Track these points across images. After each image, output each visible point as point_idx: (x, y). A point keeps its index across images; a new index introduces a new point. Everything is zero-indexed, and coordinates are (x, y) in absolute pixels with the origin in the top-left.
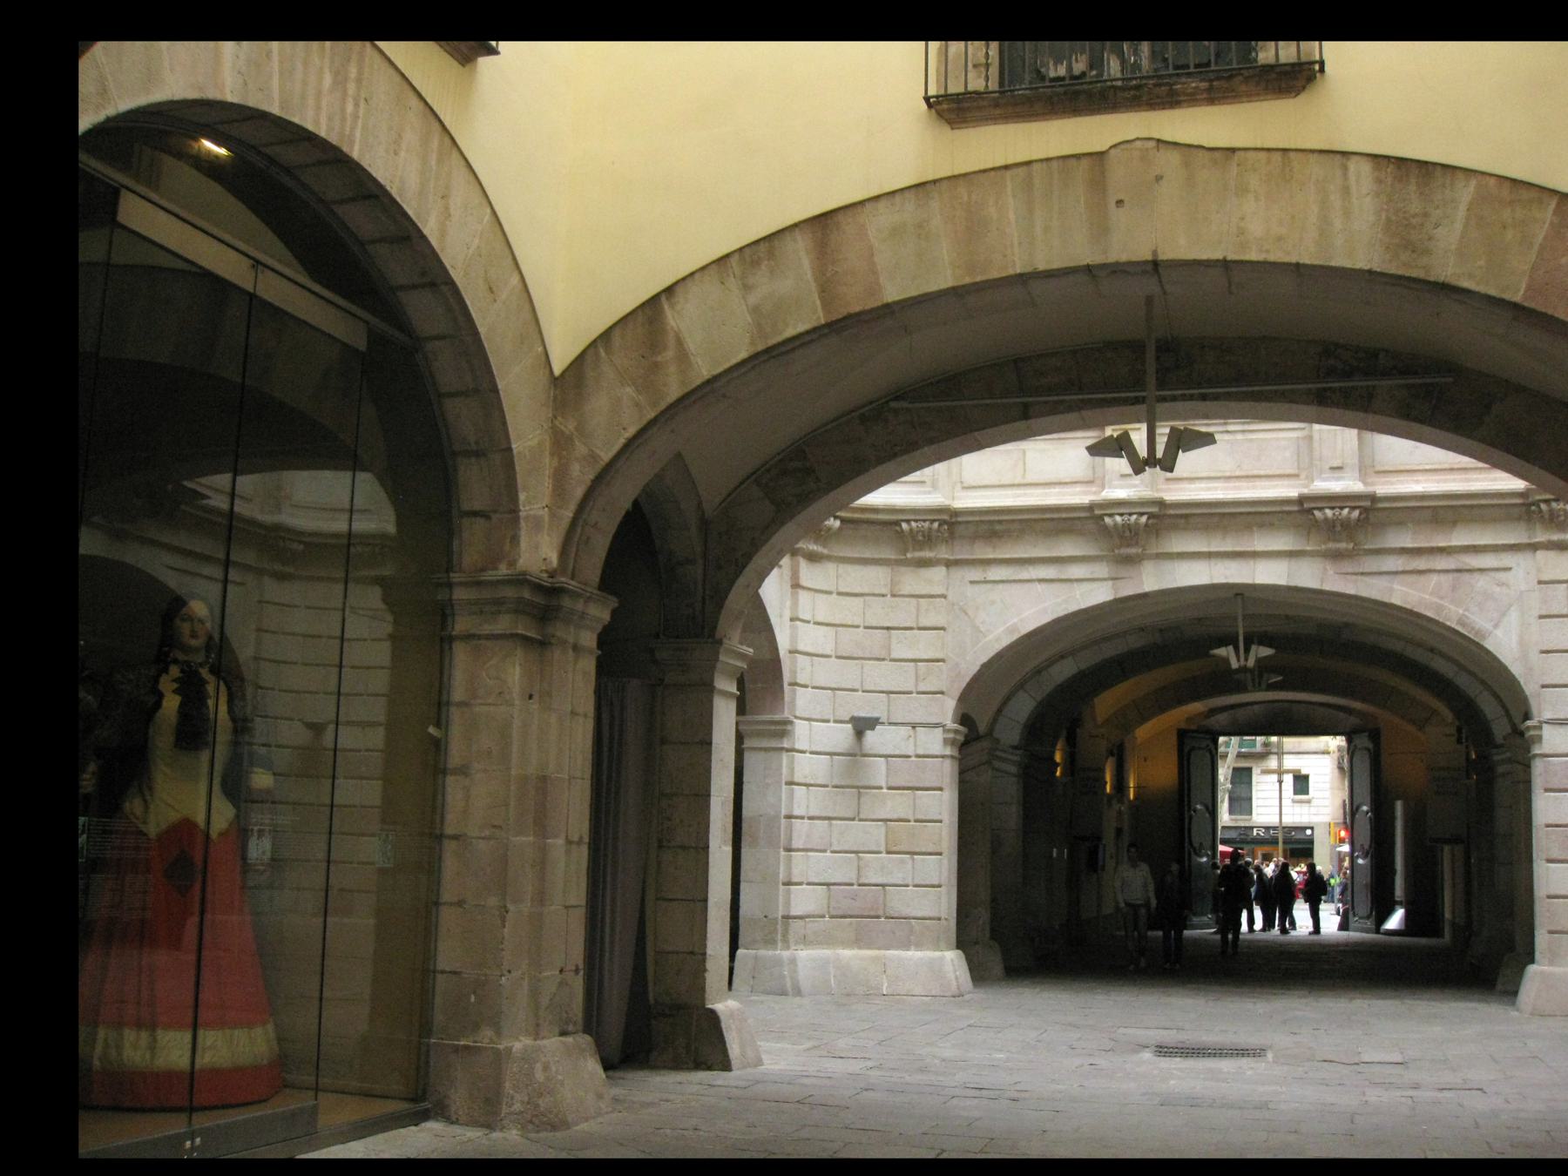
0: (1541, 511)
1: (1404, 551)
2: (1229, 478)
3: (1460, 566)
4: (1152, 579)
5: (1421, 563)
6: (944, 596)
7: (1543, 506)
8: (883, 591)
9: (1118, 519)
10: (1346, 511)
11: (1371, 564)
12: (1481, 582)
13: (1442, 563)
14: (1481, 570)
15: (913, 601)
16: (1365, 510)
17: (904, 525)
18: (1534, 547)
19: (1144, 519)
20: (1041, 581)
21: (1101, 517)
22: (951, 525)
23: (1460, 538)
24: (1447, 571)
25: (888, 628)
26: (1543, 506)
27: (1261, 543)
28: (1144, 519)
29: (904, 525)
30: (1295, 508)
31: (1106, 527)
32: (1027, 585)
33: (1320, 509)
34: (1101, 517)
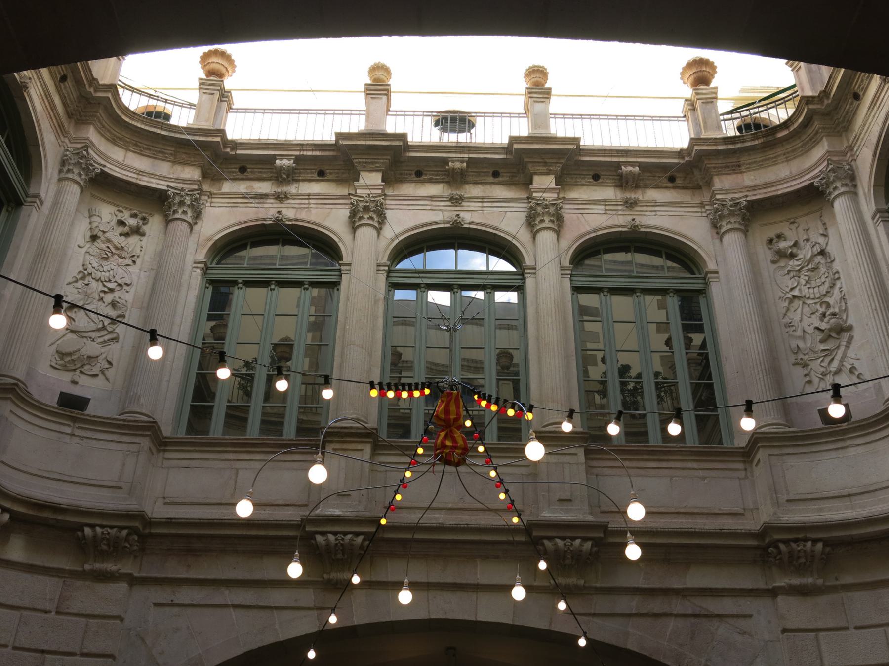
0: (780, 552)
2: (450, 509)
3: (697, 611)
5: (657, 605)
6: (121, 619)
7: (782, 547)
8: (48, 607)
9: (331, 537)
10: (578, 541)
12: (722, 630)
13: (678, 606)
15: (83, 620)
16: (597, 542)
17: (87, 531)
18: (773, 593)
19: (360, 539)
20: (235, 606)
21: (312, 536)
22: (143, 538)
25: (43, 651)
26: (782, 547)
28: (360, 539)
29: (87, 531)
30: (522, 538)
31: (317, 546)
33: (550, 538)
34: (312, 536)
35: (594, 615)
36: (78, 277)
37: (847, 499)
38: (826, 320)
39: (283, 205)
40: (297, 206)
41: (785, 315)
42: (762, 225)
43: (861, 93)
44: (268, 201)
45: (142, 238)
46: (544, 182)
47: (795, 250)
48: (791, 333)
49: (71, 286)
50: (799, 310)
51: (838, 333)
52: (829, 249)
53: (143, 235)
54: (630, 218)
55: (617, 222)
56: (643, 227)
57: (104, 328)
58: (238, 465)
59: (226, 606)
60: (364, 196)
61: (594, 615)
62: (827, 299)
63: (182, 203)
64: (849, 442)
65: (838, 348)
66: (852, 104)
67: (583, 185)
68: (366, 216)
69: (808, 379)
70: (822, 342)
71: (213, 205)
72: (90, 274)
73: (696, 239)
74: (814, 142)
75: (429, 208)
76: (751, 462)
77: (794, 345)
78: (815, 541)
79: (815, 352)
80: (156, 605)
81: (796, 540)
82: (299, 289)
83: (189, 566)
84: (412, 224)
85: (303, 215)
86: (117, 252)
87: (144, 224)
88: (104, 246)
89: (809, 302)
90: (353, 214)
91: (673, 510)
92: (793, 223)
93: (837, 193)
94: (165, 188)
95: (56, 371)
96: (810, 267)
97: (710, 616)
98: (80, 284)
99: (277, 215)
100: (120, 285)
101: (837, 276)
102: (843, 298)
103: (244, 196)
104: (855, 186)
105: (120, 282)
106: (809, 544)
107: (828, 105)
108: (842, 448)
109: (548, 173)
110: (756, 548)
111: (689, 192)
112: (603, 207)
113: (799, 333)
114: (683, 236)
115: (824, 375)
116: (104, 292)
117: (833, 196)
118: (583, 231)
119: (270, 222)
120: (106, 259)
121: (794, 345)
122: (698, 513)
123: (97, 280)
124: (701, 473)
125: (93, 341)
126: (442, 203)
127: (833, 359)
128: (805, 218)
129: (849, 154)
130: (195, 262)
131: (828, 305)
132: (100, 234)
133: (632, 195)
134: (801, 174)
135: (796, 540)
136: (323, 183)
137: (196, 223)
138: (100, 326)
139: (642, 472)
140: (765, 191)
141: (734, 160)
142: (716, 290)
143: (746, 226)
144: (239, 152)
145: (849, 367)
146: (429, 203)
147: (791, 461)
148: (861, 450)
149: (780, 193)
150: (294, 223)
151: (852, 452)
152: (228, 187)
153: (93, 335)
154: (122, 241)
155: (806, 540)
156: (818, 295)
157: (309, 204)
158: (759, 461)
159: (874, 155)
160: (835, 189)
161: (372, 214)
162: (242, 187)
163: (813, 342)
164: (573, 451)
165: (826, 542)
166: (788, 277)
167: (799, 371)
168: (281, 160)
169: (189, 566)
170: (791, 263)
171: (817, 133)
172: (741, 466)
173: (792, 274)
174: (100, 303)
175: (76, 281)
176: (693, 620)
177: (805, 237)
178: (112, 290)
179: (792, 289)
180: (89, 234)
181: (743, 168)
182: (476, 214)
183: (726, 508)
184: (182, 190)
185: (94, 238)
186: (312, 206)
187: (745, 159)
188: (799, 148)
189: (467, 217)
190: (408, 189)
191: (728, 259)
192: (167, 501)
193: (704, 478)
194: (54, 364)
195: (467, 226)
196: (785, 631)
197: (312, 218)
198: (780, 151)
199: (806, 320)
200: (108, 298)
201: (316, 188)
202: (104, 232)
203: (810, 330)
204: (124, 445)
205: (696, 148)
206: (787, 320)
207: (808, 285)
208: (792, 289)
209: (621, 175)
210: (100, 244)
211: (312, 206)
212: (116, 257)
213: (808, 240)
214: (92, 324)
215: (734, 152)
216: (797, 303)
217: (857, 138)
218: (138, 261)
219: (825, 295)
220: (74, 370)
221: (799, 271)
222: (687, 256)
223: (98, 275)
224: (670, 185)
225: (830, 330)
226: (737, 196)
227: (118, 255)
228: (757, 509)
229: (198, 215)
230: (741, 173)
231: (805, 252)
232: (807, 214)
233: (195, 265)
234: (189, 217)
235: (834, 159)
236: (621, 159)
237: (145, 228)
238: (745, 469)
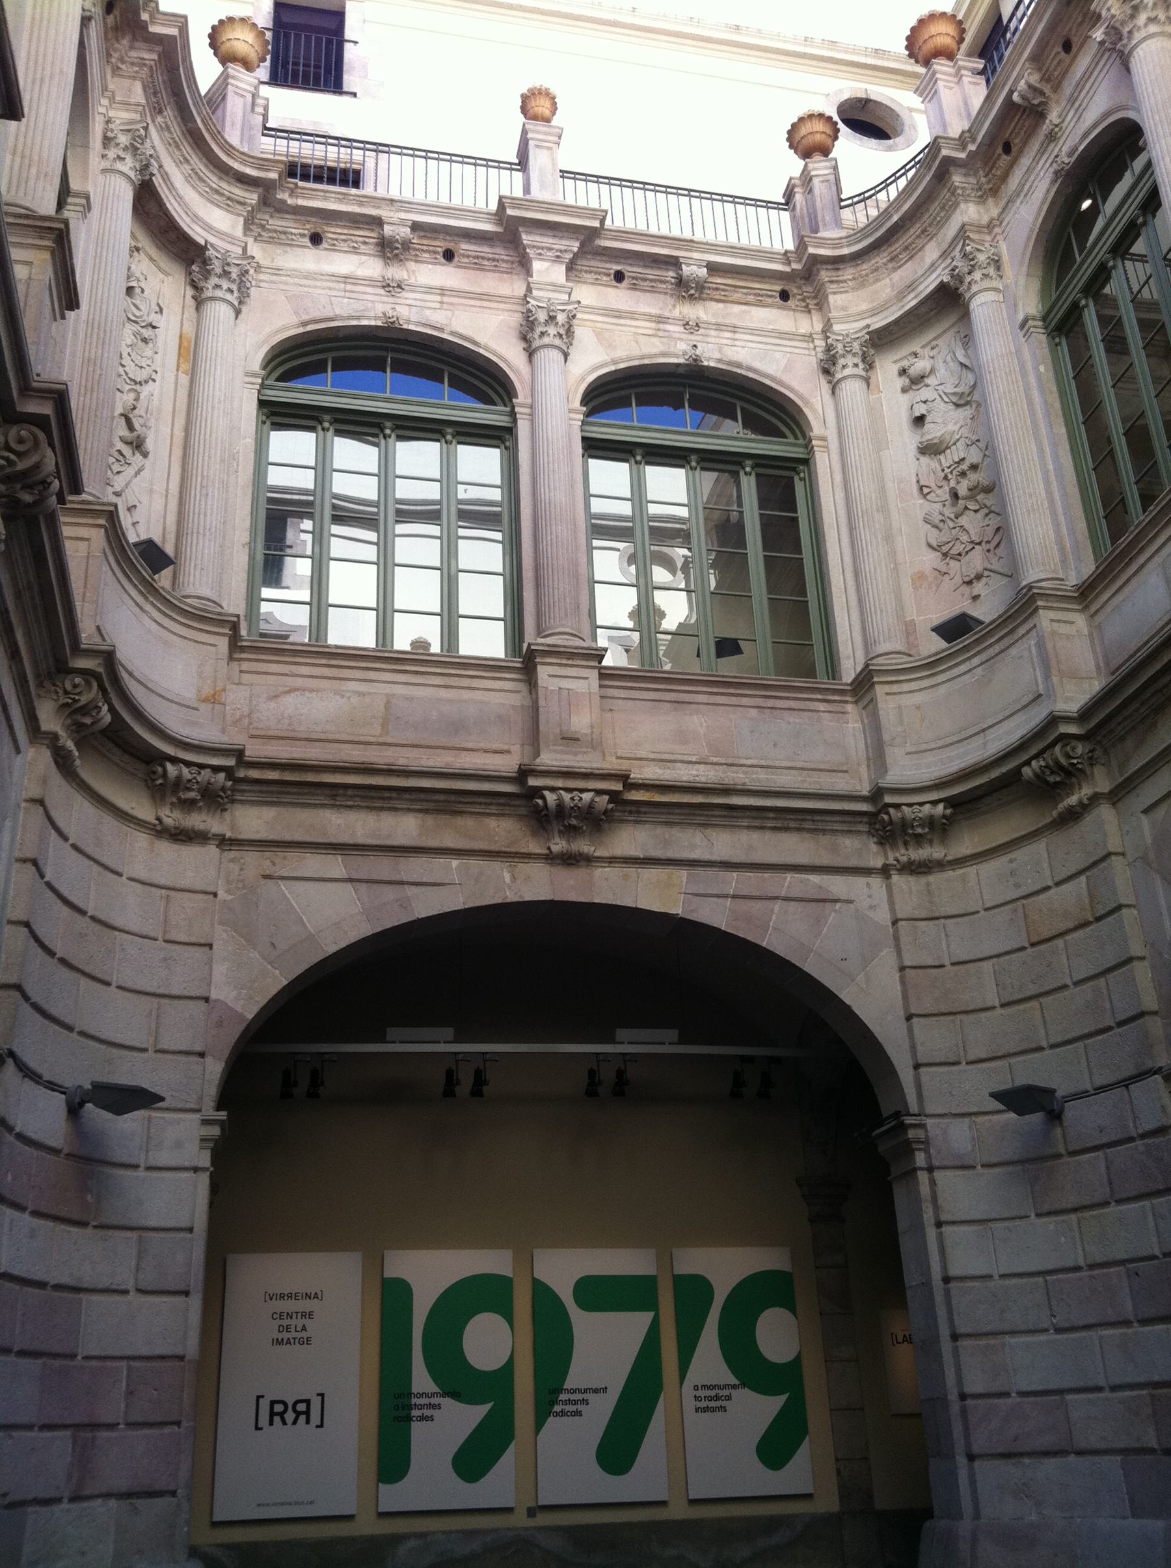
43: (325, 245)
66: (303, 235)
74: (230, 204)
93: (229, 297)
107: (284, 202)
117: (219, 293)
149: (168, 205)
160: (230, 291)
171: (243, 204)
188: (209, 186)
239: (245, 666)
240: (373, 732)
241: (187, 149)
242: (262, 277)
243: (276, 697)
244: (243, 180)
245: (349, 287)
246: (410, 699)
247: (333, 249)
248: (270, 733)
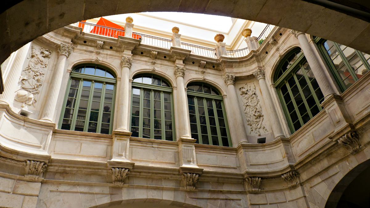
1: (210, 191)
4: (126, 195)
5: (215, 196)
8: (10, 190)
10: (194, 175)
11: (200, 195)
12: (233, 203)
13: (222, 196)
14: (233, 200)
20: (81, 193)
23: (226, 188)
24: (223, 199)
27: (165, 184)
32: (75, 194)
35: (198, 198)
36: (27, 69)
37: (266, 165)
38: (257, 113)
39: (98, 56)
40: (103, 57)
41: (245, 110)
42: (238, 84)
43: (268, 52)
44: (93, 54)
45: (49, 59)
46: (179, 63)
47: (247, 92)
48: (247, 115)
49: (24, 72)
50: (249, 109)
51: (260, 117)
52: (256, 93)
53: (49, 58)
54: (203, 76)
55: (199, 77)
56: (206, 79)
57: (34, 88)
58: (82, 141)
59: (77, 192)
60: (126, 57)
61: (198, 198)
62: (256, 107)
63: (65, 50)
64: (266, 149)
65: (260, 121)
67: (189, 64)
68: (127, 64)
69: (252, 129)
70: (255, 119)
71: (74, 52)
72: (30, 69)
73: (221, 85)
74: (253, 62)
75: (145, 64)
76: (238, 153)
77: (248, 119)
78: (259, 178)
79: (253, 122)
80: (51, 191)
81: (254, 177)
82: (102, 84)
83: (64, 177)
84: (140, 69)
85: (105, 60)
86: (41, 62)
87: (50, 54)
88: (36, 60)
89: (251, 107)
90: (122, 62)
91: (218, 166)
92: (246, 84)
93: (260, 78)
94: (60, 44)
95: (16, 102)
96: (252, 97)
97: (230, 200)
98: (27, 72)
99: (97, 59)
100: (40, 74)
101: (259, 101)
102: (261, 107)
103: (85, 51)
104: (265, 77)
105: (41, 73)
106: (257, 178)
107: (259, 54)
108: (264, 150)
109: (181, 59)
110: (242, 179)
111: (218, 71)
112: (195, 72)
113: (249, 116)
114: (217, 84)
115: (256, 128)
116: (35, 76)
117: (259, 79)
118: (190, 78)
119: (94, 61)
120: (37, 64)
121: (248, 119)
122: (224, 167)
123: (33, 71)
124: (225, 155)
125: (30, 92)
126: (149, 63)
127: (258, 124)
128: (249, 83)
129: (263, 68)
130: (68, 70)
131: (257, 109)
132: (35, 55)
133: (204, 70)
134: (249, 71)
135: (254, 177)
136: (111, 51)
137: (68, 57)
138: (33, 87)
139: (209, 153)
140: (239, 74)
141: (231, 64)
142: (226, 101)
143: (234, 83)
144: (85, 36)
145: (263, 127)
146: (145, 63)
147: (251, 153)
148: (269, 151)
149: (243, 75)
150: (102, 62)
151: (267, 151)
152: (79, 47)
153: (31, 90)
154: (43, 59)
155: (256, 177)
156: (254, 106)
157: (107, 57)
158: (241, 152)
159: (272, 69)
160: (260, 77)
161: (128, 63)
162: (84, 48)
163: (253, 119)
164: (191, 146)
165: (262, 178)
166: (245, 99)
167: (249, 127)
168: (99, 41)
169: (64, 177)
170: (246, 95)
171: (255, 60)
172: (235, 154)
173: (246, 99)
174: (33, 80)
175: (25, 71)
176: (225, 201)
177: (250, 89)
178: (37, 75)
179: (247, 103)
180: (31, 55)
181: (233, 67)
182: (159, 68)
183: (232, 166)
184: (66, 45)
185: (33, 56)
186: (108, 57)
187: (234, 65)
189: (156, 69)
190: (138, 57)
191: (229, 92)
192: (56, 152)
193: (226, 157)
194: (16, 100)
195: (157, 72)
196: (252, 204)
197: (108, 61)
198: (244, 64)
199: (251, 112)
200: (36, 78)
201: (109, 52)
202: (37, 55)
203: (252, 115)
204: (43, 131)
205: (222, 59)
206: (245, 112)
207: (251, 102)
208: (247, 103)
209: (200, 63)
210: (35, 58)
211: (108, 57)
212: (40, 64)
213: (250, 90)
214: (31, 86)
215: (232, 62)
216: (248, 107)
217: (266, 64)
218: (47, 67)
219: (255, 106)
220: (23, 102)
221: (248, 98)
222: (217, 90)
223: (33, 69)
224: (213, 68)
225: (258, 116)
226: (232, 74)
227: (41, 63)
228: (240, 167)
229: (69, 53)
230: (233, 68)
231: (250, 93)
232: (250, 82)
233: (68, 71)
234: (67, 54)
235: (260, 68)
236: (201, 59)
237: (50, 56)
238: (236, 155)
239: (292, 143)
240: (313, 143)
241: (241, 64)
242: (265, 67)
243: (298, 146)
244: (251, 58)
245: (274, 56)
246: (315, 131)
247: (270, 51)
248: (301, 154)
